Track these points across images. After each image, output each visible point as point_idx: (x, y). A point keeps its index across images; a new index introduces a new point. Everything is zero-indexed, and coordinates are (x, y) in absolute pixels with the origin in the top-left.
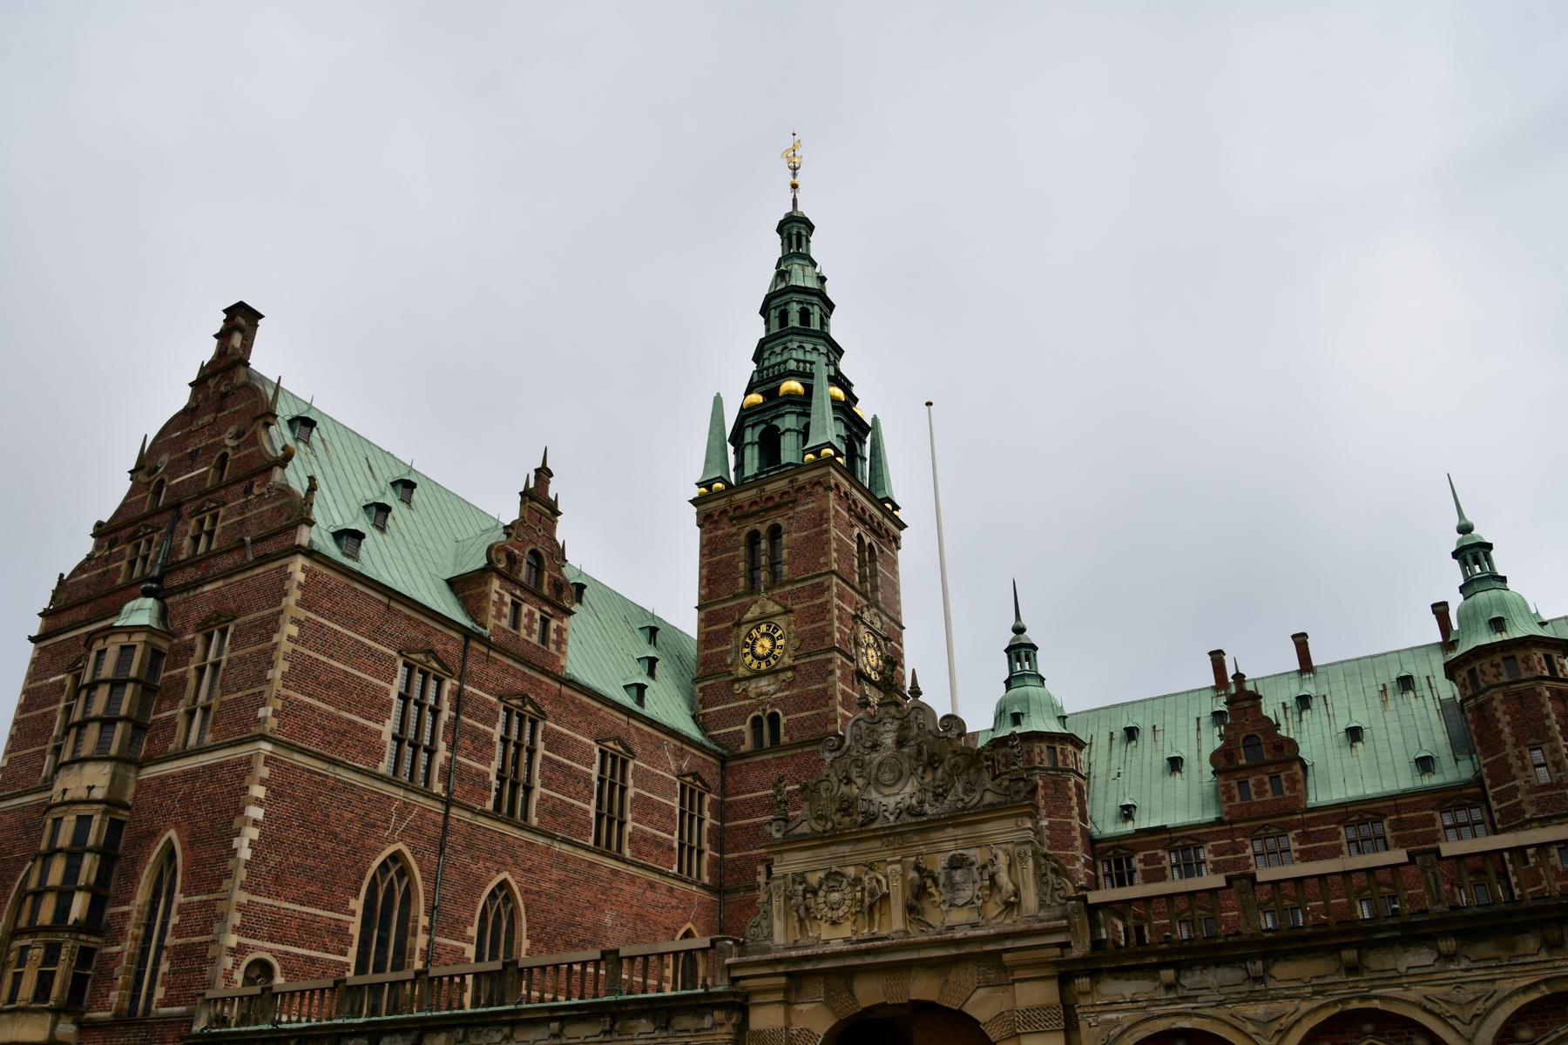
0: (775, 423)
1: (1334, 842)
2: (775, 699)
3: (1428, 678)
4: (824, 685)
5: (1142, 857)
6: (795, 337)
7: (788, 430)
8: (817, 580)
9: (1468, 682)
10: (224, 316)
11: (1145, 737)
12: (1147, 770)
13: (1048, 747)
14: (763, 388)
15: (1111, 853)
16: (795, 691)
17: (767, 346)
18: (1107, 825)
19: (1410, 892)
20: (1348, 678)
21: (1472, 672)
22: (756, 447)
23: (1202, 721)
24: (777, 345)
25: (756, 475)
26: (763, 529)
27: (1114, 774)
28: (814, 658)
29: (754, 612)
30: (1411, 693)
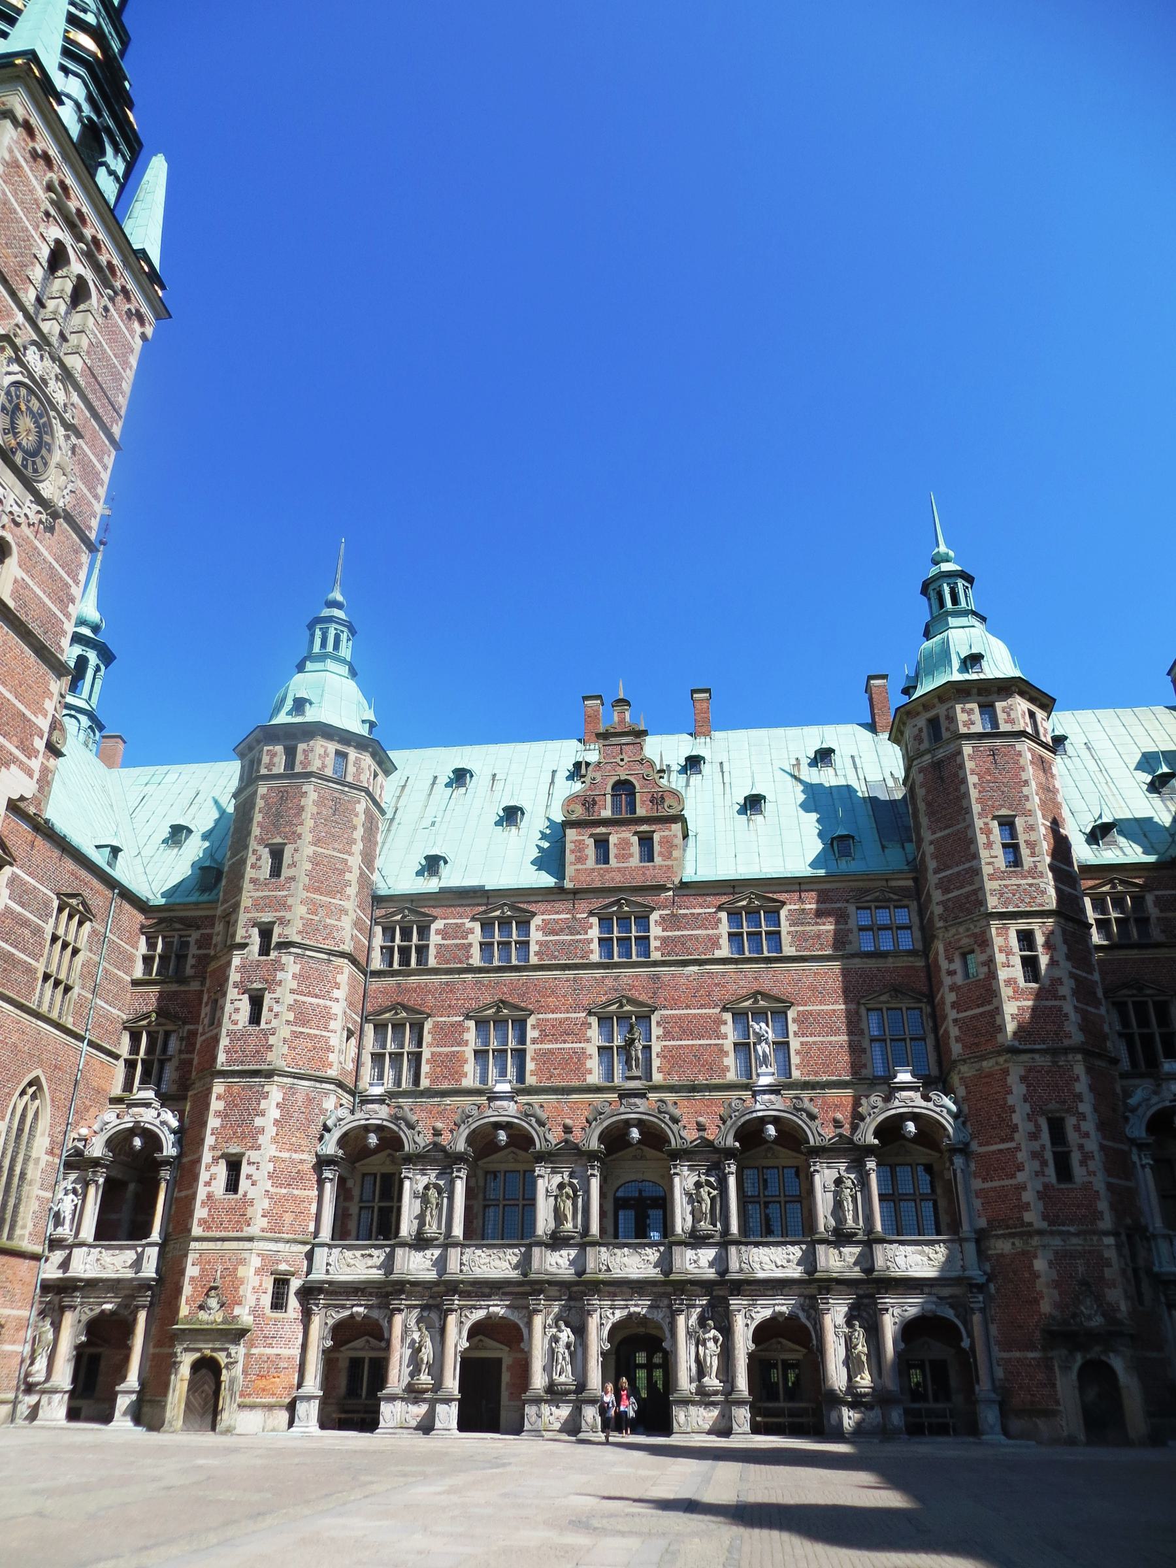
1: (710, 932)
3: (852, 757)
5: (442, 927)
9: (925, 734)
13: (338, 753)
19: (801, 1008)
23: (558, 775)
27: (427, 822)
30: (830, 770)
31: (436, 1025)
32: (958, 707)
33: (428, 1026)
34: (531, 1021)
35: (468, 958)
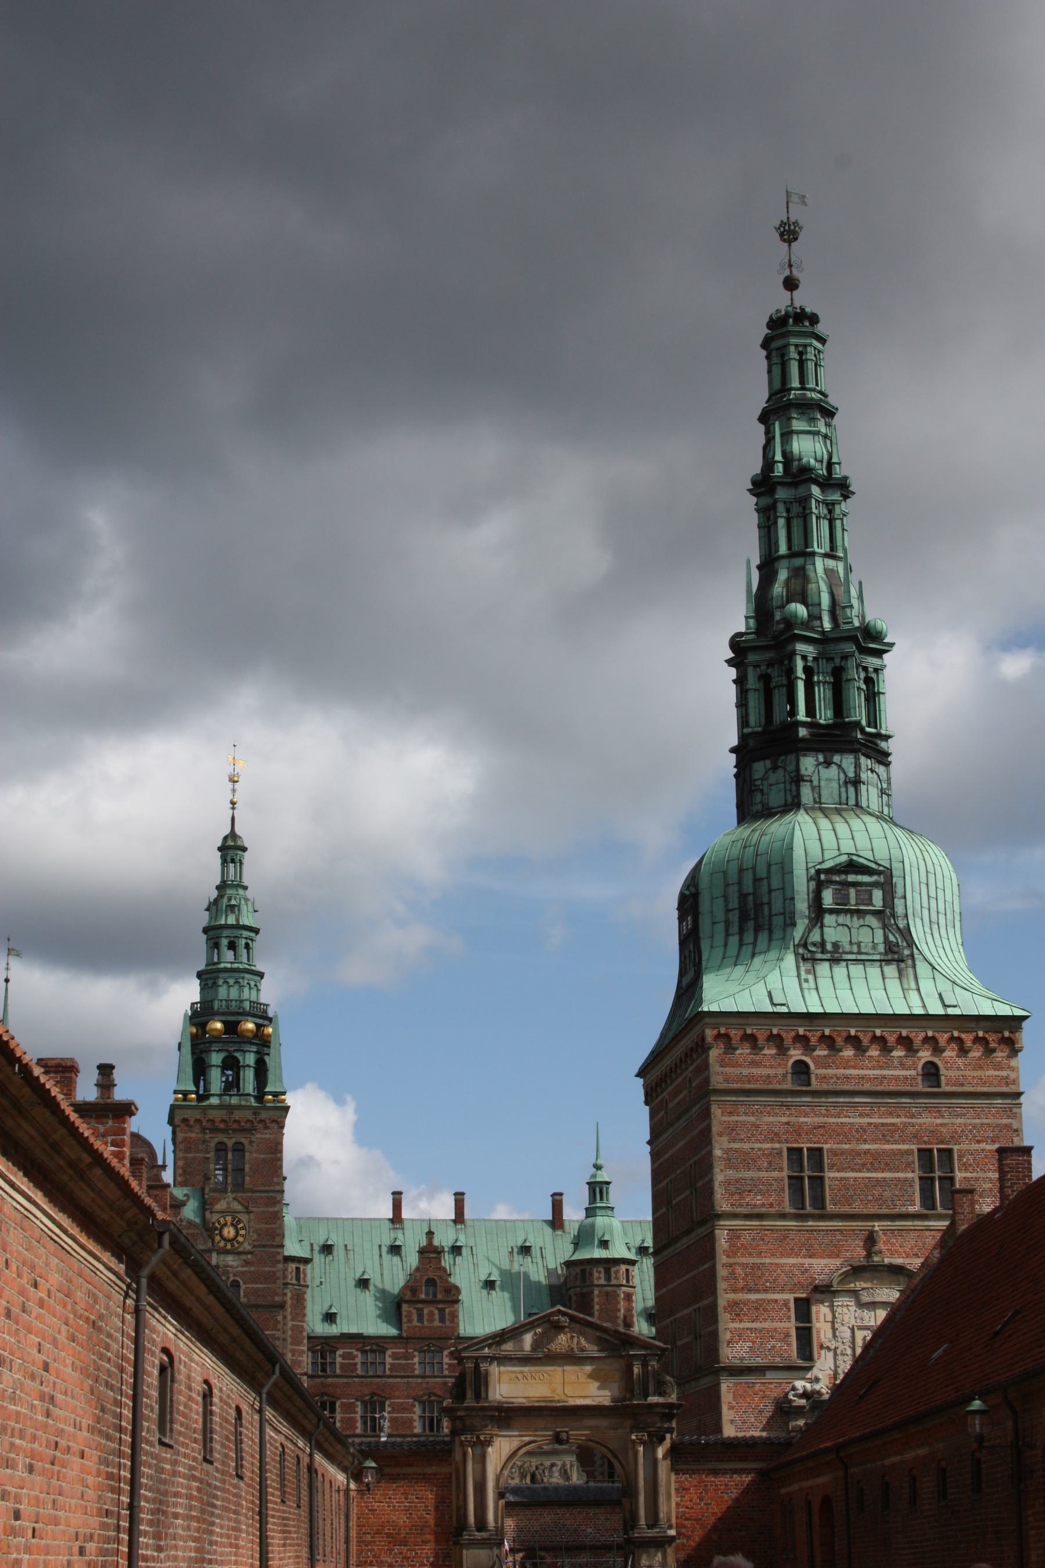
0: (237, 1054)
2: (238, 1272)
3: (541, 1248)
4: (273, 1269)
6: (247, 976)
7: (249, 1066)
8: (271, 1194)
9: (579, 1276)
10: (98, 1071)
11: (339, 1252)
12: (342, 1283)
14: (224, 1018)
15: (319, 1347)
16: (252, 1269)
17: (222, 975)
18: (321, 1329)
20: (488, 1236)
21: (583, 1271)
22: (219, 1069)
24: (230, 977)
25: (220, 1096)
26: (230, 1143)
27: (317, 1282)
28: (267, 1249)
29: (221, 1205)
31: (342, 1403)
32: (595, 1270)
33: (338, 1404)
34: (387, 1403)
35: (356, 1369)
